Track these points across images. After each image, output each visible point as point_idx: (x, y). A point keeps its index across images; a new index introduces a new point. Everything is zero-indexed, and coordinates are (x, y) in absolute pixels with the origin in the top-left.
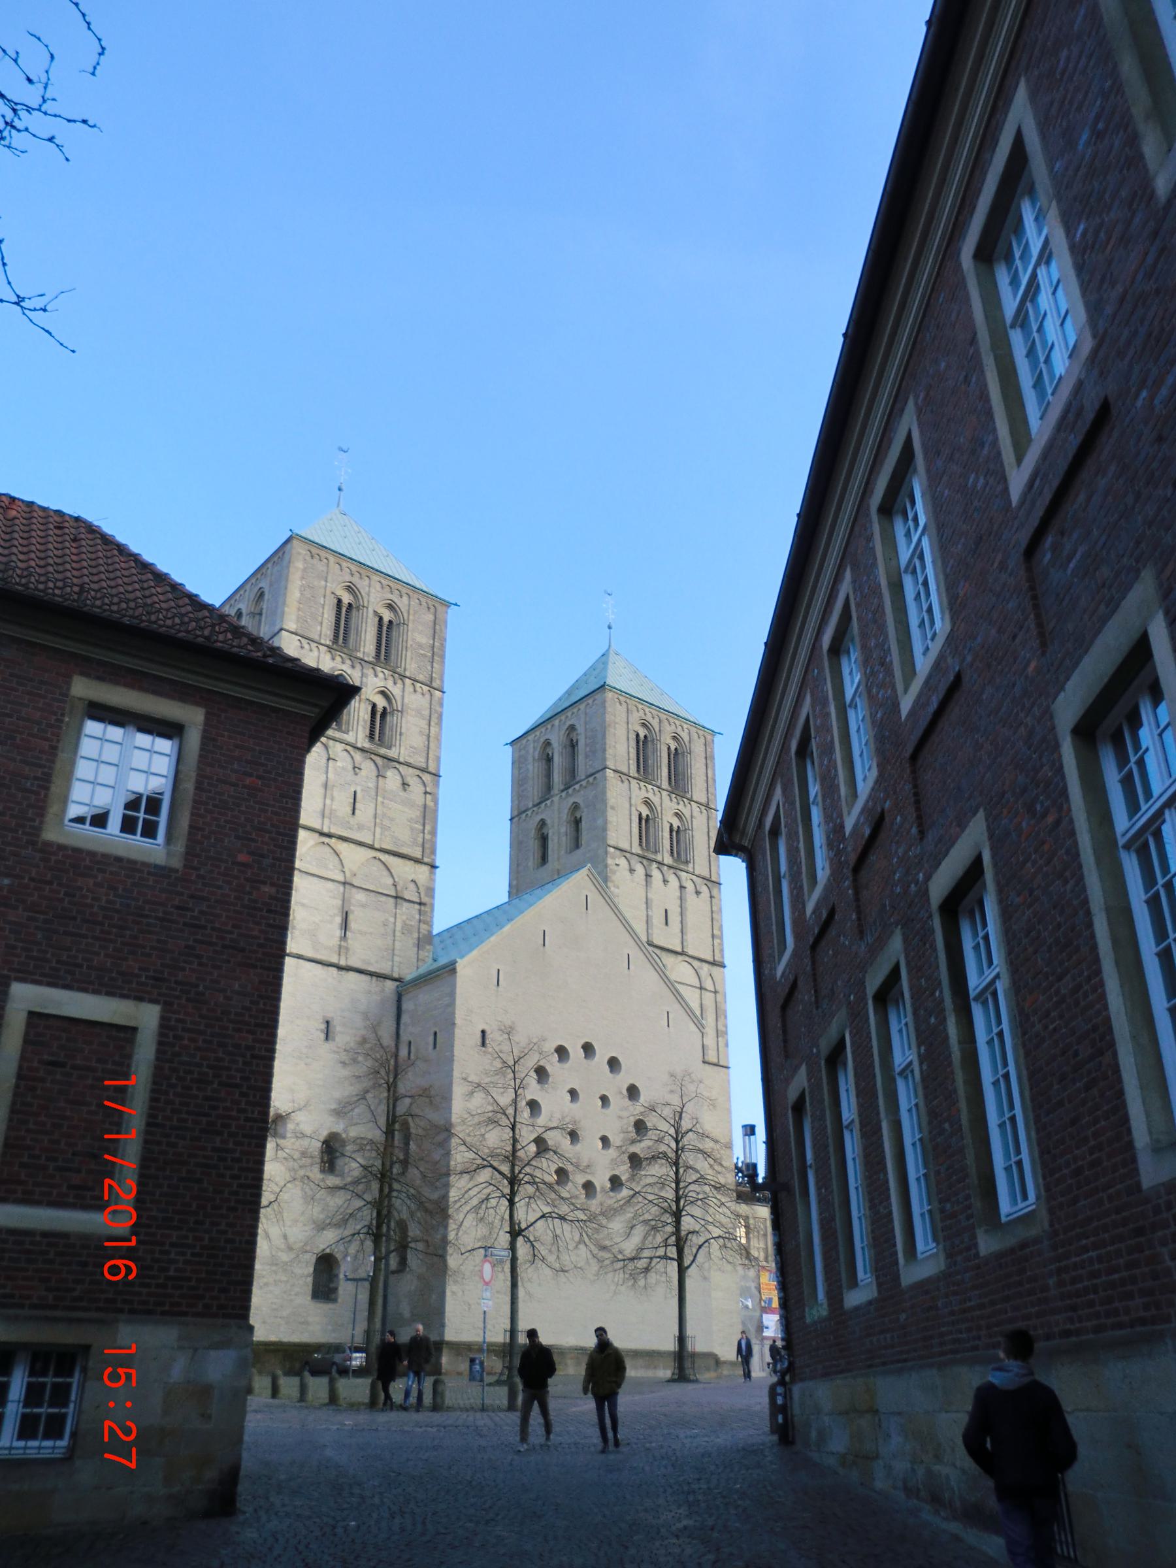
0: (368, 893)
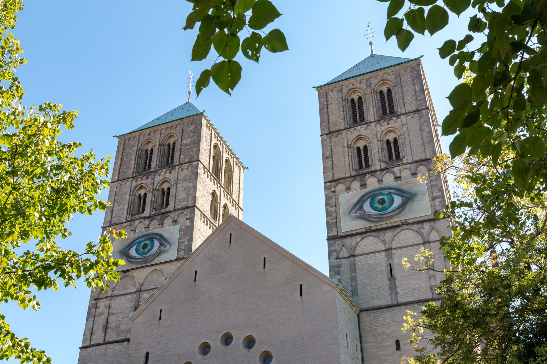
0: (150, 291)
